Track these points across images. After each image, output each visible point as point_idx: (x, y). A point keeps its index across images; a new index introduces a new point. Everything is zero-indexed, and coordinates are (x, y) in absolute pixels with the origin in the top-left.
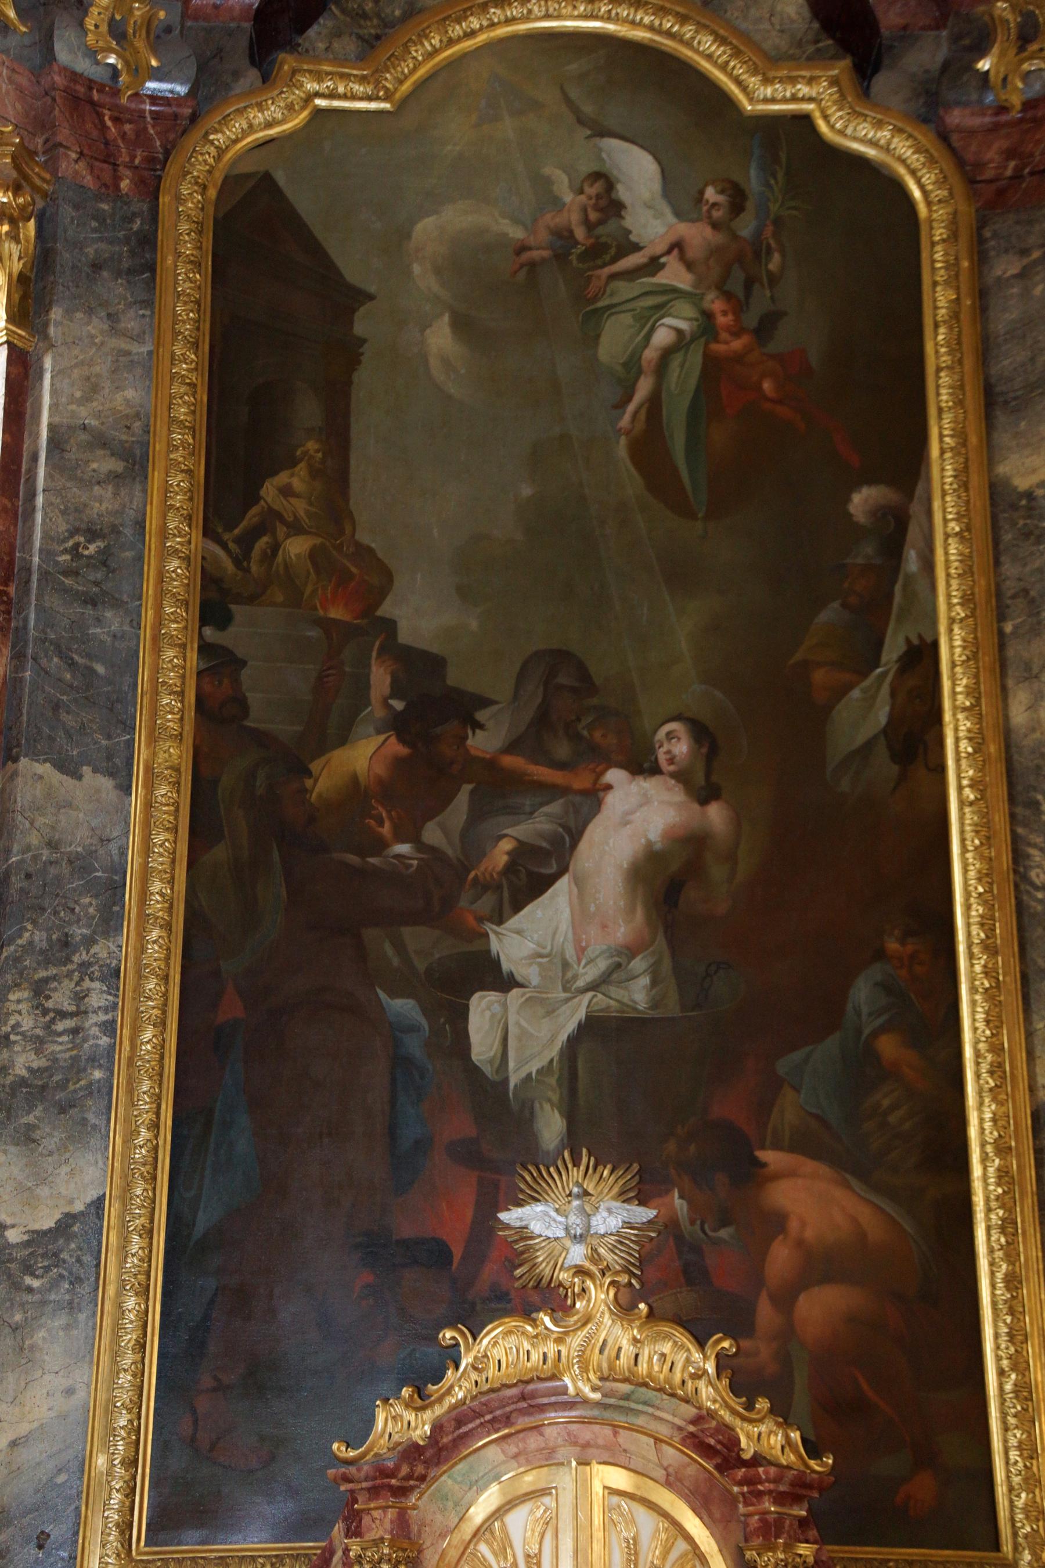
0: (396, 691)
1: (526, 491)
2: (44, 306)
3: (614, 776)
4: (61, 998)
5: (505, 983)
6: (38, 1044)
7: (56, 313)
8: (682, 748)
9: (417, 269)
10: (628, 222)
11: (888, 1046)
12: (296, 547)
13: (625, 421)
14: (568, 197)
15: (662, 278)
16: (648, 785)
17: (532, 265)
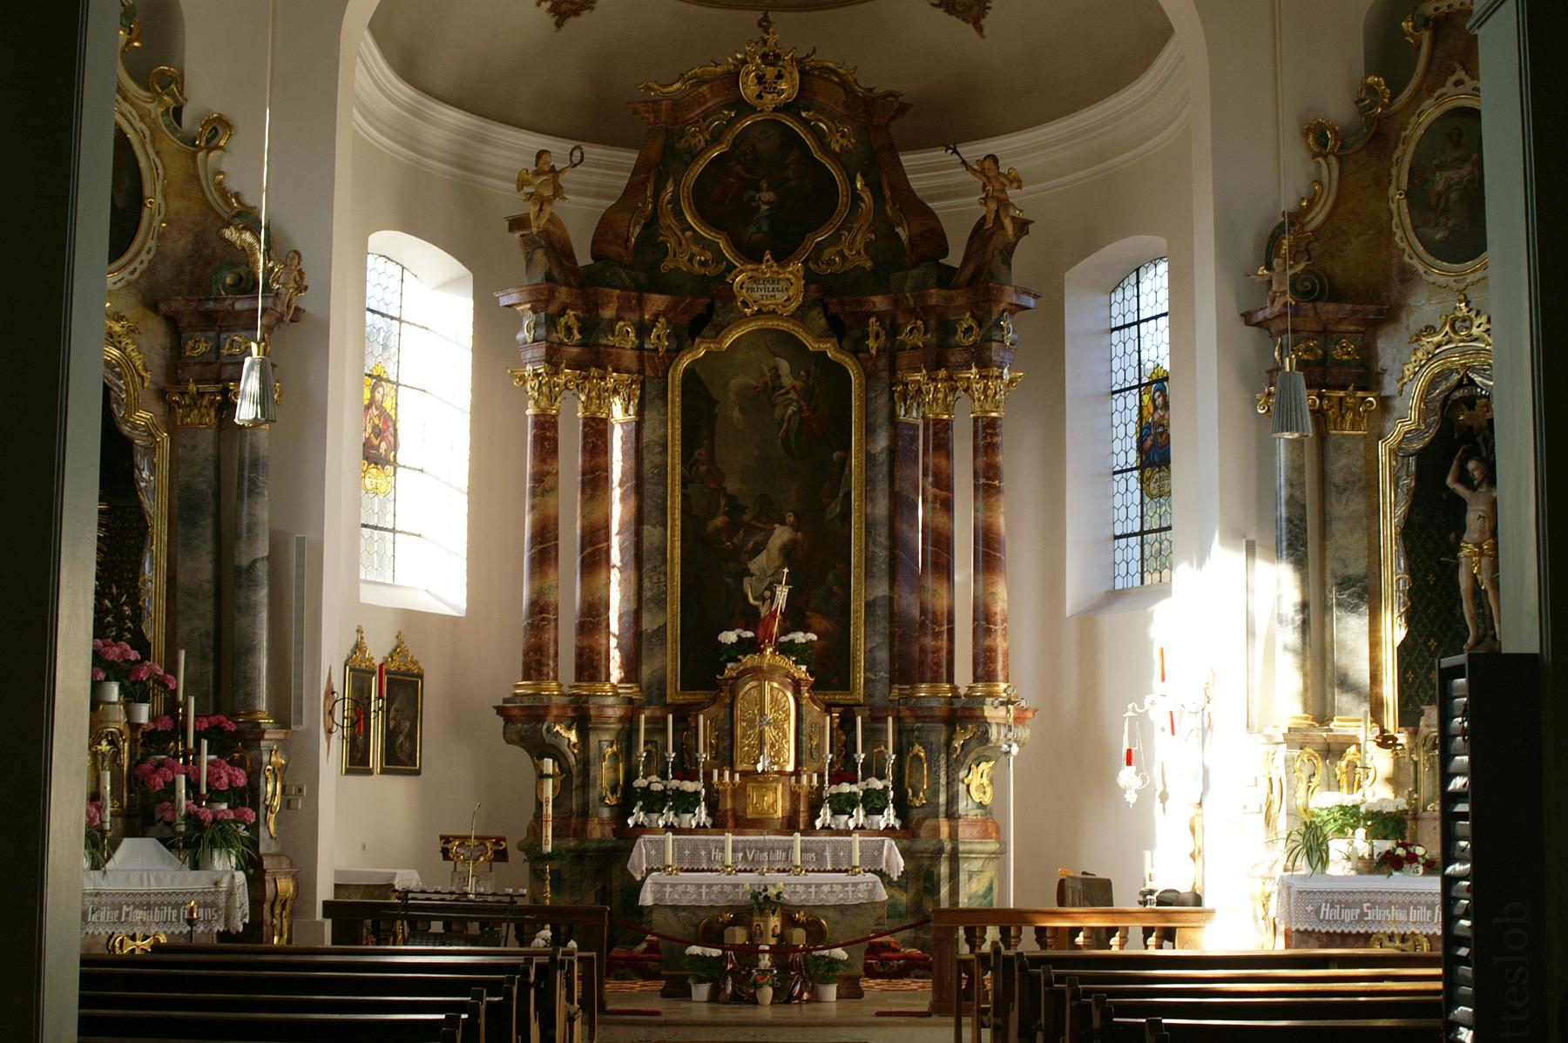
0: (727, 506)
1: (756, 453)
2: (644, 411)
3: (777, 526)
4: (655, 580)
5: (752, 575)
6: (651, 590)
7: (646, 412)
8: (792, 519)
9: (730, 394)
10: (782, 380)
11: (835, 589)
12: (703, 468)
13: (780, 435)
14: (767, 373)
15: (790, 396)
16: (783, 528)
17: (758, 393)
